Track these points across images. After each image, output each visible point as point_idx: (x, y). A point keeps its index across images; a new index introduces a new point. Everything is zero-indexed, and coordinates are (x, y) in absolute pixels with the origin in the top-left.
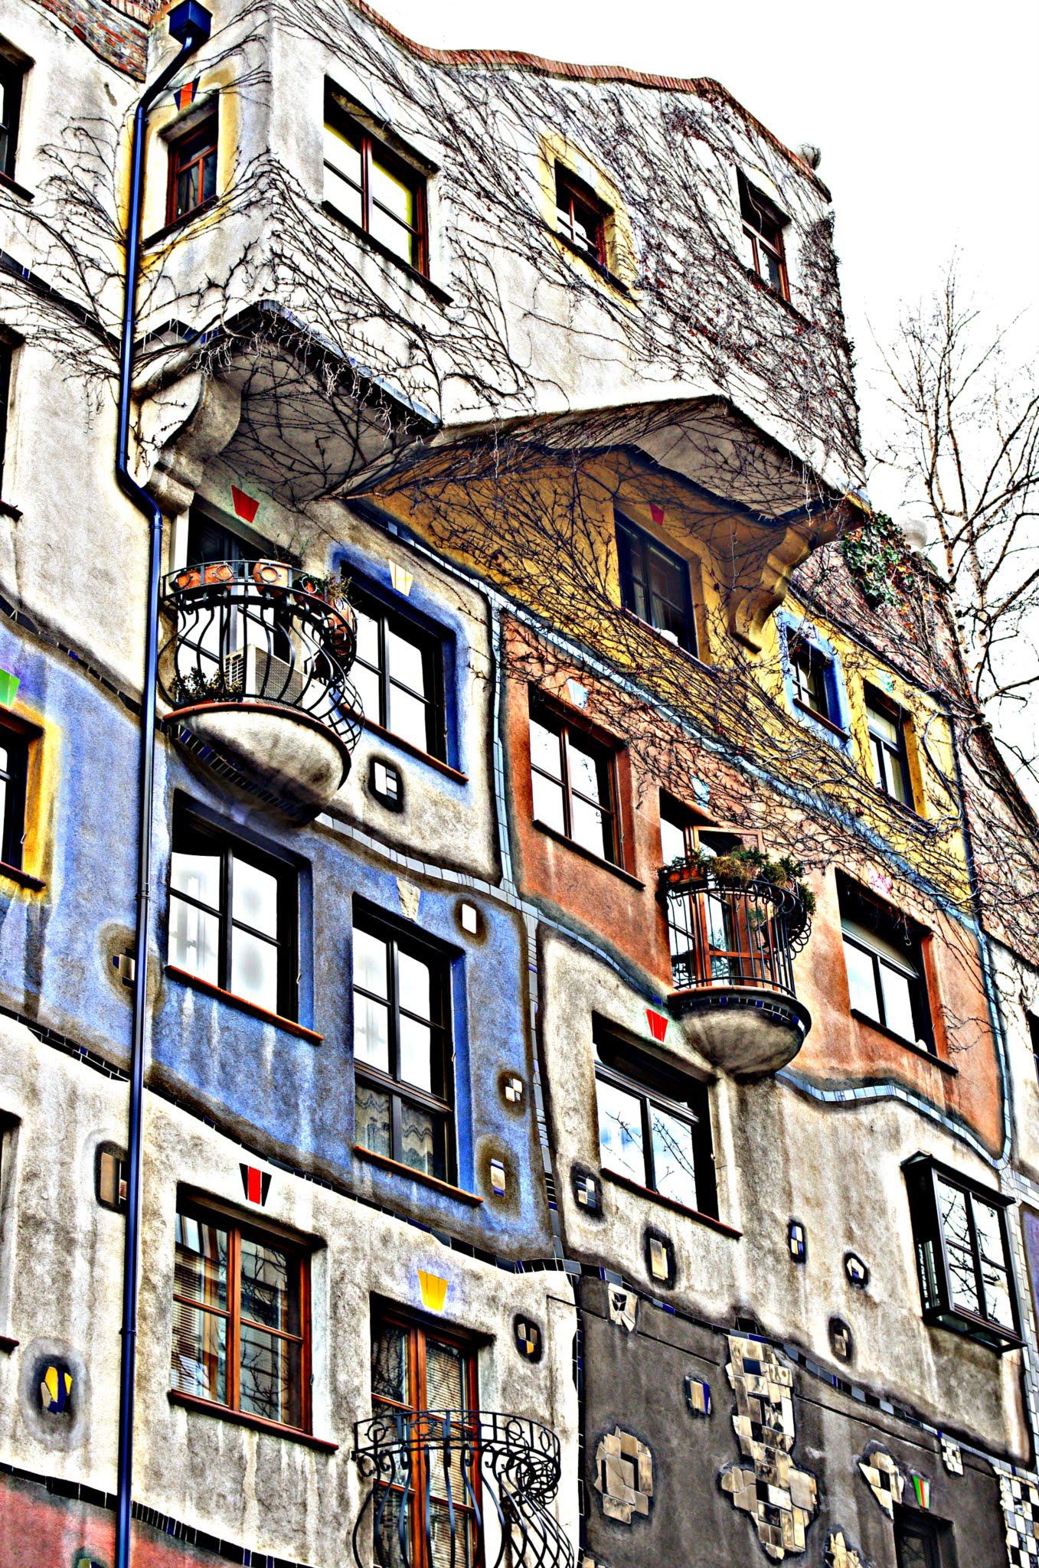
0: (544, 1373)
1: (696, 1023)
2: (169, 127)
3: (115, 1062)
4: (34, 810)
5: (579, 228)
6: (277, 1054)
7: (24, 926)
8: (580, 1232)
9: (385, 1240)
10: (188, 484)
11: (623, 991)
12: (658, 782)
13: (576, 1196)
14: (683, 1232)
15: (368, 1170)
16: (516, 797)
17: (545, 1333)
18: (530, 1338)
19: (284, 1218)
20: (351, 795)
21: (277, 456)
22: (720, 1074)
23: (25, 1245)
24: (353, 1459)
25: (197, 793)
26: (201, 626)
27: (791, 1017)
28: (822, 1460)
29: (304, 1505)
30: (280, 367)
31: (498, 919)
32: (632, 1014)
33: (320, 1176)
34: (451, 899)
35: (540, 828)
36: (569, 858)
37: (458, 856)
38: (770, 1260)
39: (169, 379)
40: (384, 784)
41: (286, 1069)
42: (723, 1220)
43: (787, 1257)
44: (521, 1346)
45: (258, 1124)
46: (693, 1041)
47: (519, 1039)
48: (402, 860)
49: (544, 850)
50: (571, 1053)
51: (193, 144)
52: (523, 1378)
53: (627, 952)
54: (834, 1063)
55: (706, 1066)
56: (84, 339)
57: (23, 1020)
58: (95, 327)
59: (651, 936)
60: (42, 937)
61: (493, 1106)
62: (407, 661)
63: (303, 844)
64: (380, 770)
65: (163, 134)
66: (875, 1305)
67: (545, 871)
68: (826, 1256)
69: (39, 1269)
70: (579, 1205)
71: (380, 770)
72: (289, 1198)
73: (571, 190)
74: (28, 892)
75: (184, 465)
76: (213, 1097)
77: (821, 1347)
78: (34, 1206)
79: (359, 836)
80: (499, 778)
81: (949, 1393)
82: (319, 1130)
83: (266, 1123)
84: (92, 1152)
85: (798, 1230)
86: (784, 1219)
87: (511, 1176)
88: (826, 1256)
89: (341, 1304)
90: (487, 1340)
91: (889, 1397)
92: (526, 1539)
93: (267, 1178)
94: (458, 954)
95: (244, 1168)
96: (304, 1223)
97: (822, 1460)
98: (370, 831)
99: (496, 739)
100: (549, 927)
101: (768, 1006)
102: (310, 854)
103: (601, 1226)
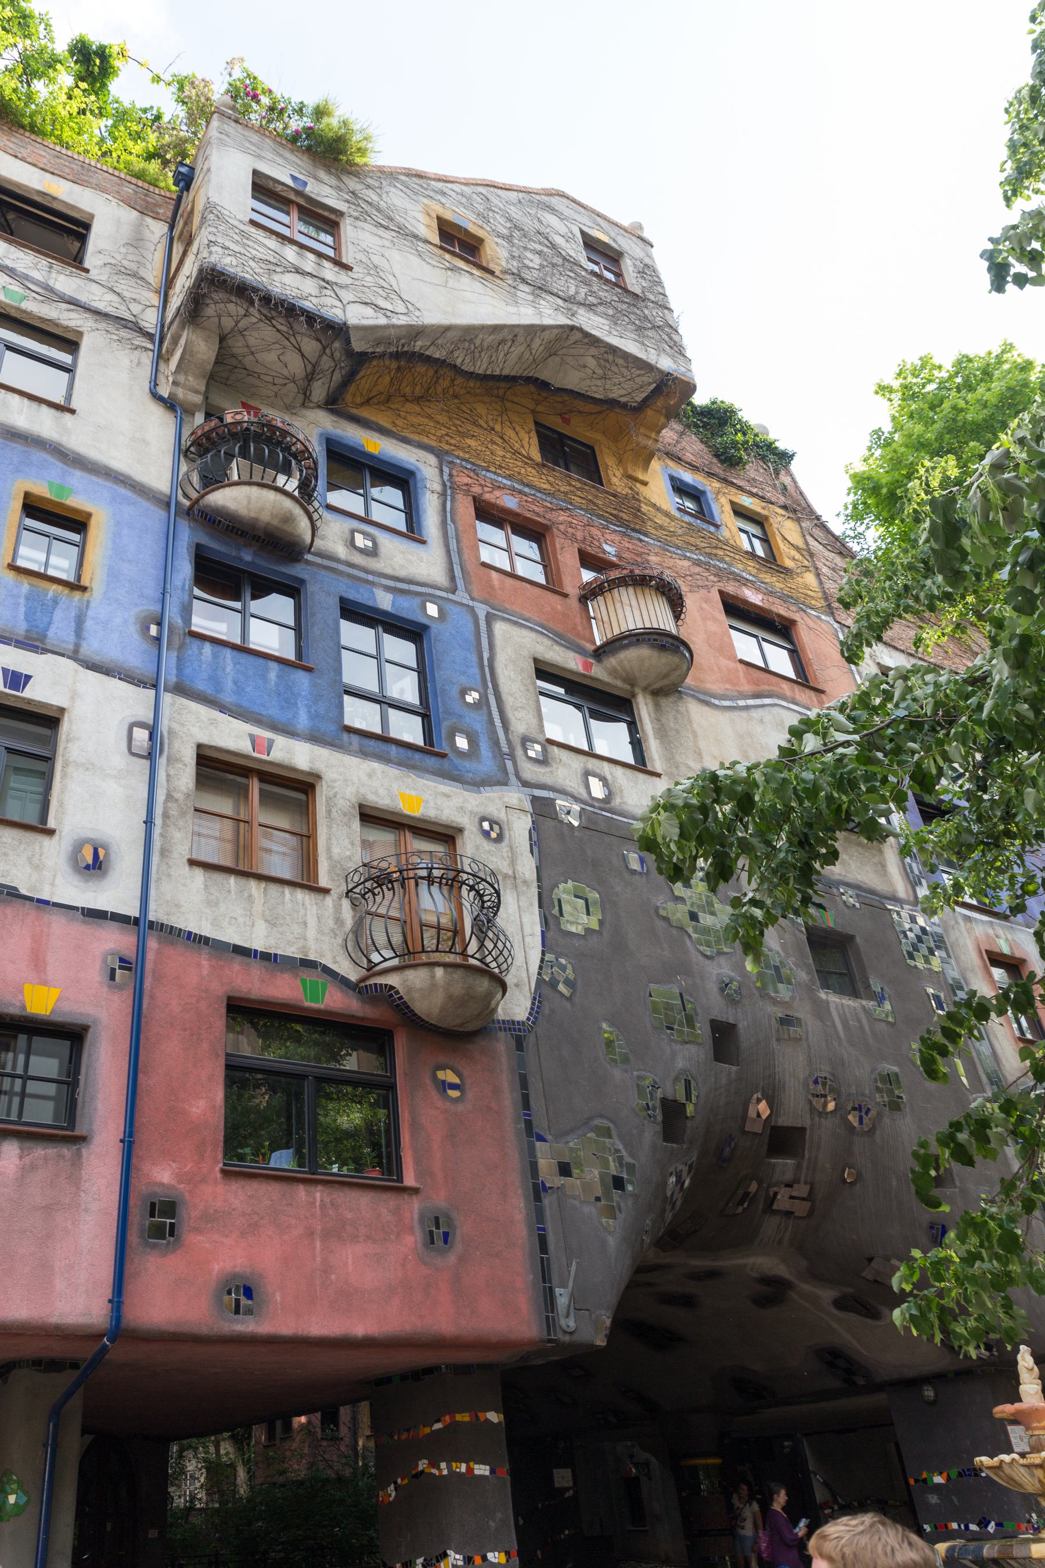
3: (145, 680)
11: (557, 648)
21: (262, 376)
24: (347, 896)
31: (453, 611)
35: (485, 565)
36: (509, 581)
49: (490, 577)
50: (514, 679)
57: (69, 657)
59: (578, 620)
67: (492, 587)
84: (126, 727)
89: (334, 810)
93: (271, 743)
101: (655, 640)
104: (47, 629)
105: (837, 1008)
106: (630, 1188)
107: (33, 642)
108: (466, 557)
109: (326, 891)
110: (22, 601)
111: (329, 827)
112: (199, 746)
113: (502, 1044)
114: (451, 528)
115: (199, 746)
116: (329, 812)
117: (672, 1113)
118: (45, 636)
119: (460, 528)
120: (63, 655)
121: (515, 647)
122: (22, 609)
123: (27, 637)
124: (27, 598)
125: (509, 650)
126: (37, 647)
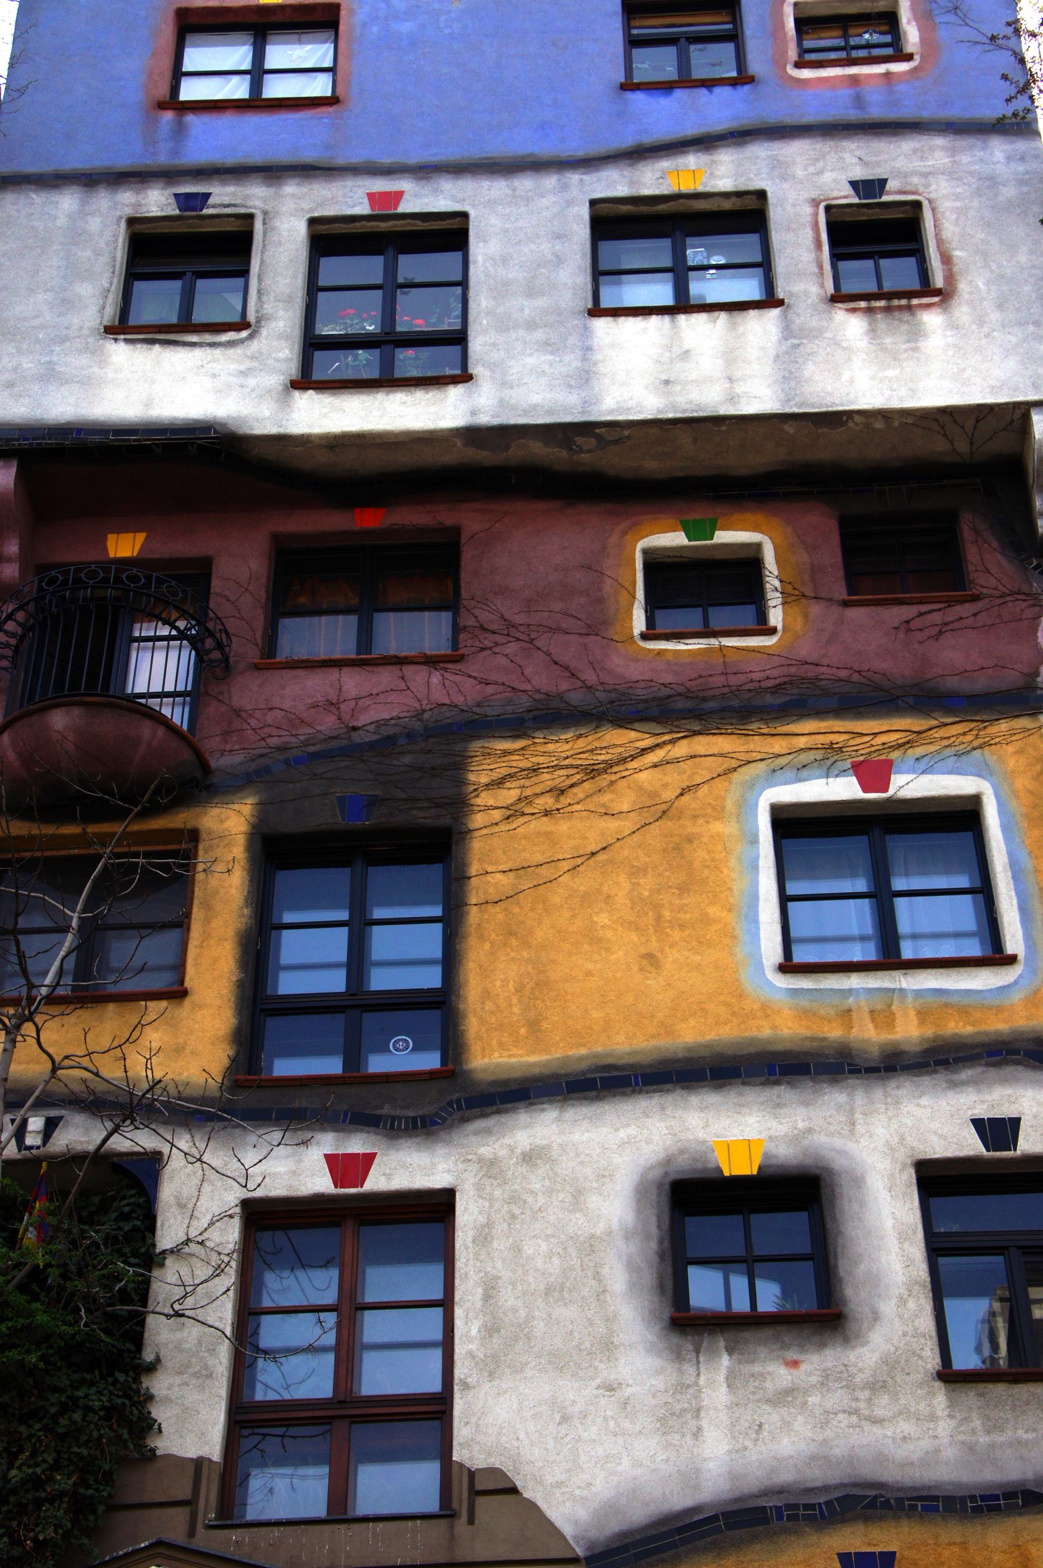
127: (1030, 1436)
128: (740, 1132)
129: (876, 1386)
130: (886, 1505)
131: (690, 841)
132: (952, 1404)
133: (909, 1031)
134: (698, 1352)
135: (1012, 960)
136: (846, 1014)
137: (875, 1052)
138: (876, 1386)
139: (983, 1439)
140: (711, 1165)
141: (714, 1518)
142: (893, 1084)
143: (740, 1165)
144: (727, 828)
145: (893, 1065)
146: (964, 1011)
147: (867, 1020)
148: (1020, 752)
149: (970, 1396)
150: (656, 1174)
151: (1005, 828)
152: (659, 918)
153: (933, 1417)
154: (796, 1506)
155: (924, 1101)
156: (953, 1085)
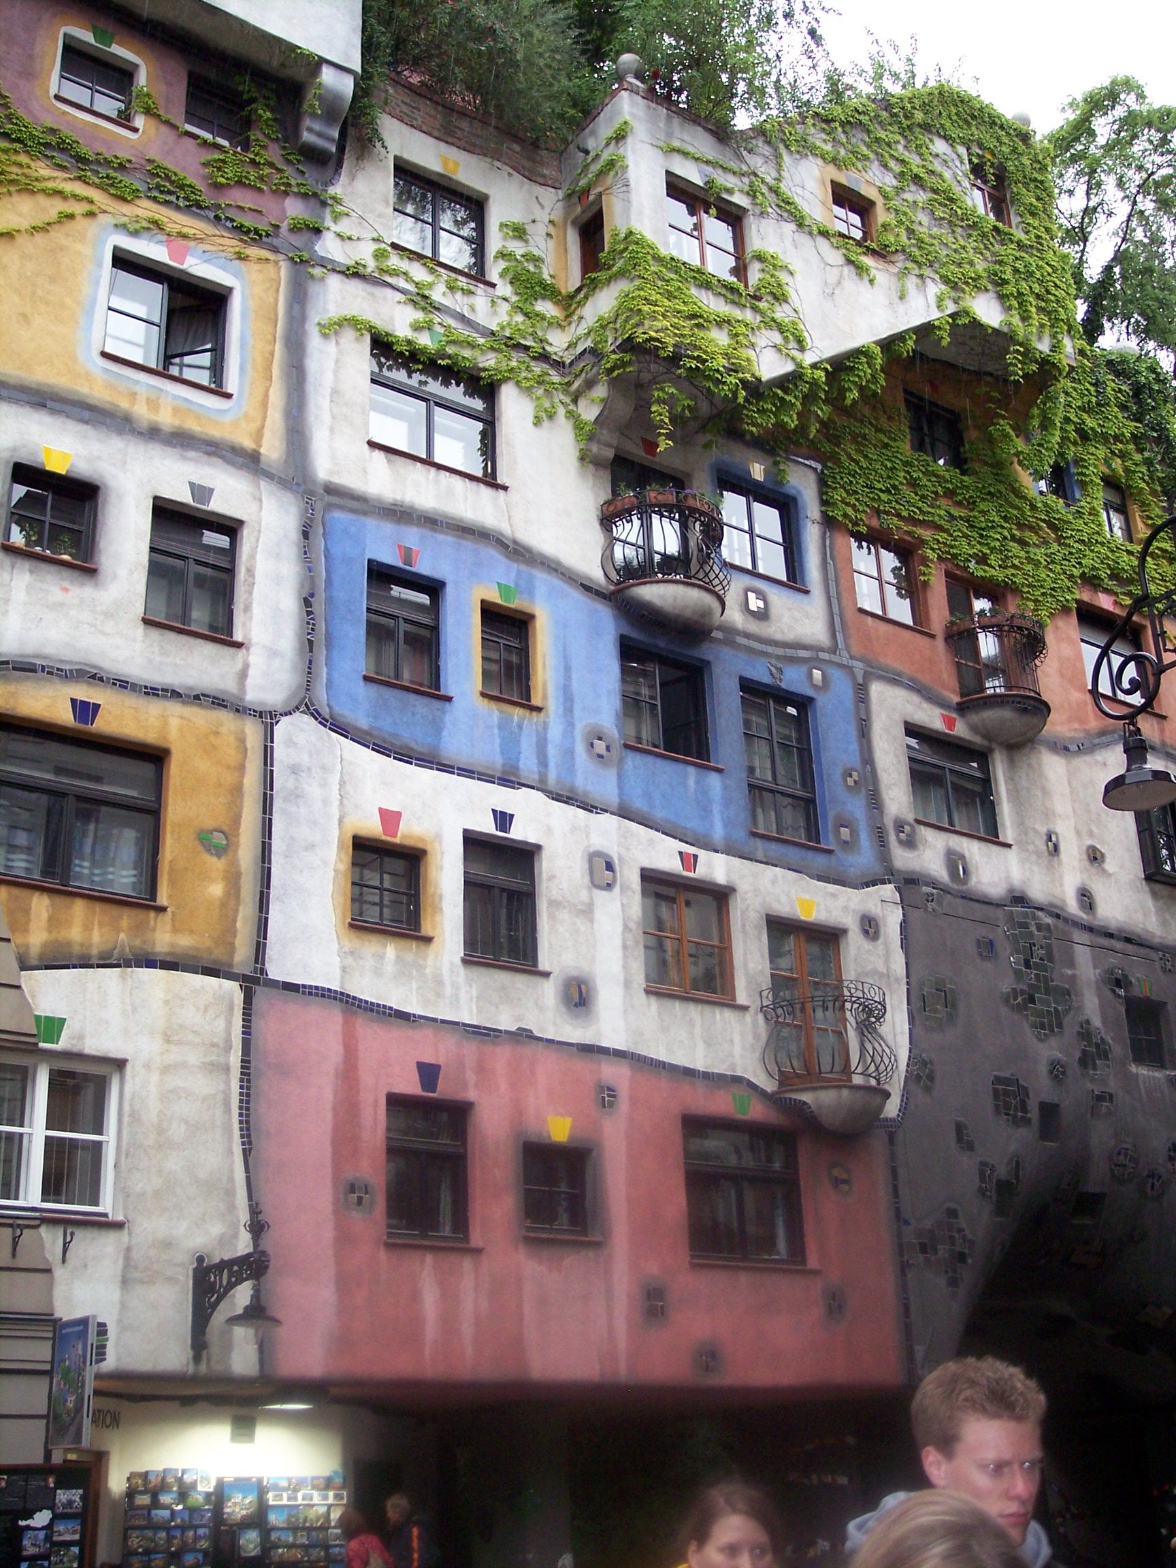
0: (881, 947)
1: (975, 718)
2: (576, 218)
4: (535, 664)
5: (855, 219)
6: (697, 783)
7: (534, 734)
8: (903, 859)
9: (774, 882)
10: (610, 446)
11: (925, 705)
12: (943, 566)
13: (898, 836)
14: (973, 850)
15: (759, 843)
16: (844, 595)
17: (881, 923)
18: (870, 927)
19: (708, 879)
20: (734, 616)
22: (994, 745)
23: (552, 917)
25: (634, 634)
26: (630, 530)
27: (1039, 708)
28: (1074, 976)
29: (732, 1041)
30: (653, 367)
32: (932, 718)
33: (730, 850)
34: (804, 669)
35: (862, 611)
36: (883, 627)
37: (807, 640)
38: (1034, 857)
39: (590, 384)
40: (755, 603)
41: (704, 792)
42: (1001, 839)
43: (1046, 854)
44: (866, 932)
45: (688, 826)
46: (974, 728)
47: (854, 746)
48: (770, 649)
51: (591, 230)
52: (868, 951)
53: (926, 679)
54: (1076, 726)
55: (986, 743)
56: (538, 368)
58: (544, 357)
60: (545, 739)
61: (840, 791)
62: (768, 519)
63: (705, 651)
64: (751, 596)
65: (573, 223)
66: (1110, 875)
68: (1072, 852)
69: (561, 929)
70: (900, 842)
71: (752, 596)
72: (709, 865)
73: (844, 197)
74: (534, 714)
75: (605, 435)
76: (659, 814)
77: (1072, 906)
78: (555, 894)
79: (741, 640)
80: (832, 584)
81: (1164, 923)
82: (725, 826)
83: (693, 824)
84: (586, 858)
85: (1054, 839)
86: (1044, 830)
87: (854, 833)
88: (1072, 852)
90: (844, 931)
91: (1120, 930)
92: (874, 1048)
93: (696, 857)
94: (811, 700)
95: (680, 853)
96: (720, 878)
97: (1074, 976)
98: (748, 636)
99: (829, 560)
100: (871, 673)
102: (710, 657)
103: (916, 853)
104: (518, 760)
105: (1144, 1082)
106: (970, 1261)
107: (508, 779)
108: (844, 601)
109: (744, 1008)
110: (496, 731)
111: (745, 942)
112: (642, 870)
113: (878, 1144)
114: (831, 568)
115: (642, 870)
116: (743, 926)
117: (1005, 1188)
118: (518, 769)
119: (839, 565)
120: (533, 788)
121: (892, 707)
122: (498, 741)
123: (503, 772)
124: (499, 728)
125: (884, 715)
126: (513, 782)
127: (182, 663)
128: (63, 448)
129: (109, 615)
130: (101, 679)
131: (61, 249)
132: (146, 635)
133: (166, 419)
134: (13, 567)
135: (229, 396)
136: (133, 395)
137: (144, 425)
138: (109, 615)
139: (158, 659)
140: (39, 460)
141: (7, 663)
142: (151, 446)
143: (57, 466)
144: (87, 250)
145: (153, 434)
146: (198, 418)
147: (144, 403)
148: (260, 271)
149: (155, 634)
150: (6, 455)
151: (243, 316)
152: (34, 293)
153: (134, 640)
154: (52, 667)
155: (166, 462)
156: (184, 458)
